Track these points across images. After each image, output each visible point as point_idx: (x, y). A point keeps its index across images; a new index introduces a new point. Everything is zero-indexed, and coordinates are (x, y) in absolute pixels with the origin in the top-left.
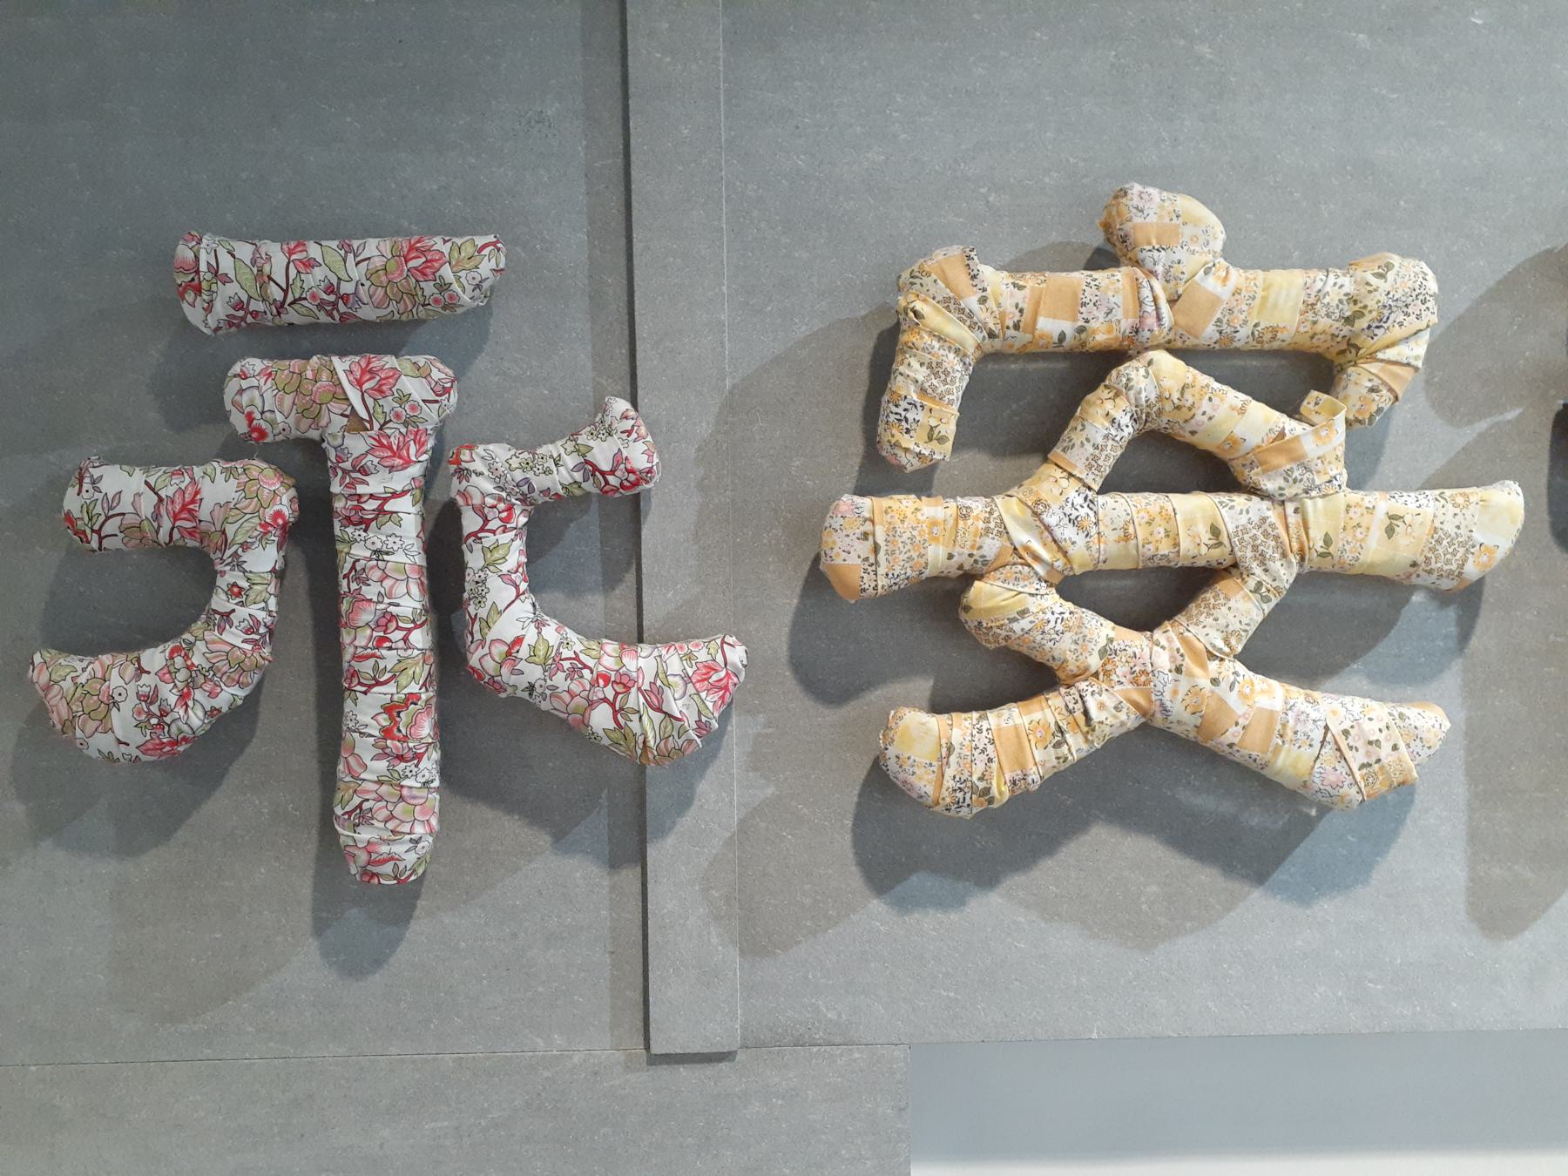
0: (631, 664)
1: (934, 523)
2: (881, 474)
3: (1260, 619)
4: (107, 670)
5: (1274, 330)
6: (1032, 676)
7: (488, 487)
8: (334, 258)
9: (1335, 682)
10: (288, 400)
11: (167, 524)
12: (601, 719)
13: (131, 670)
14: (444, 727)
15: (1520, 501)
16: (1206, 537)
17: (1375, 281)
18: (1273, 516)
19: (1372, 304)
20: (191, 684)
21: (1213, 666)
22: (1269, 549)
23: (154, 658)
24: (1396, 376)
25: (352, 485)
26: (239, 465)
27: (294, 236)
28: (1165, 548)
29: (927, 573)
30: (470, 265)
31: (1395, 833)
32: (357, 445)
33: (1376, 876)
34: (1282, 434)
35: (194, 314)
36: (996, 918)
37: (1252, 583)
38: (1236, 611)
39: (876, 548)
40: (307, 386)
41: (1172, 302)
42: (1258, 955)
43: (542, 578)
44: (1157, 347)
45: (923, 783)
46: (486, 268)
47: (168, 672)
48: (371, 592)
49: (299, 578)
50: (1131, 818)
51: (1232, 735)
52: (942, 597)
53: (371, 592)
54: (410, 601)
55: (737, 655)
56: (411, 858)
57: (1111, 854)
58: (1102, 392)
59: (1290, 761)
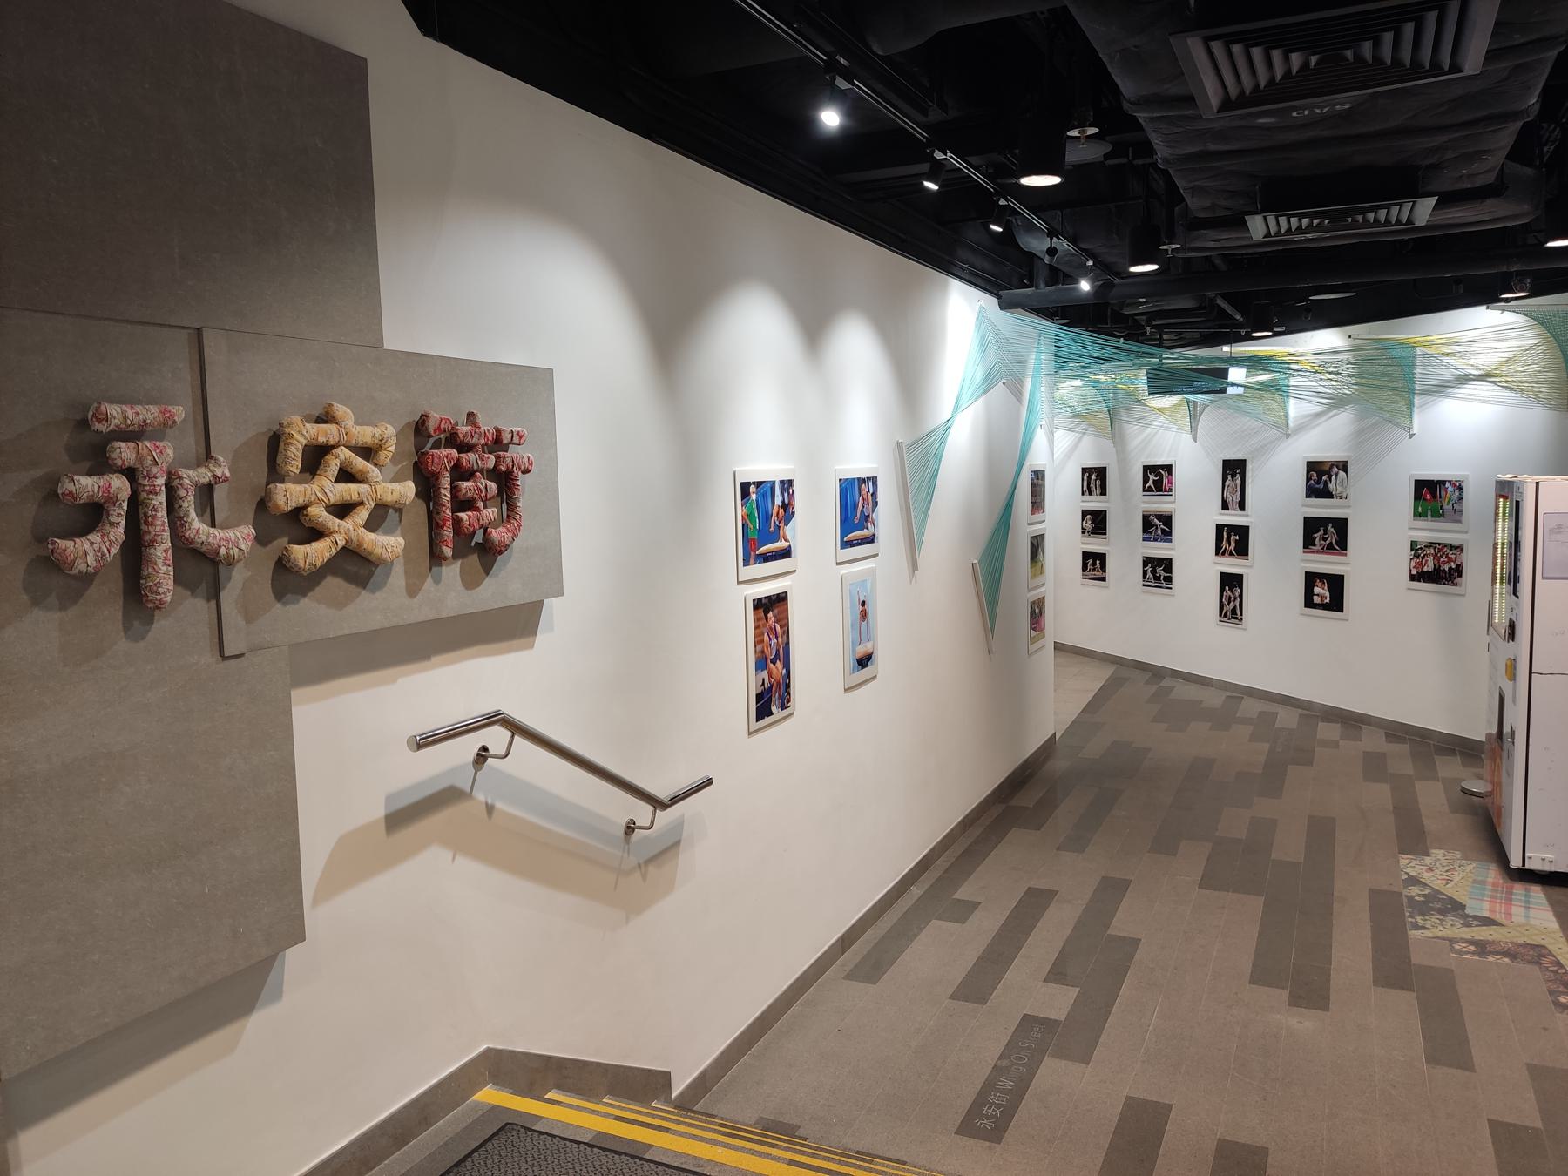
38: (362, 515)
50: (335, 574)
52: (299, 511)
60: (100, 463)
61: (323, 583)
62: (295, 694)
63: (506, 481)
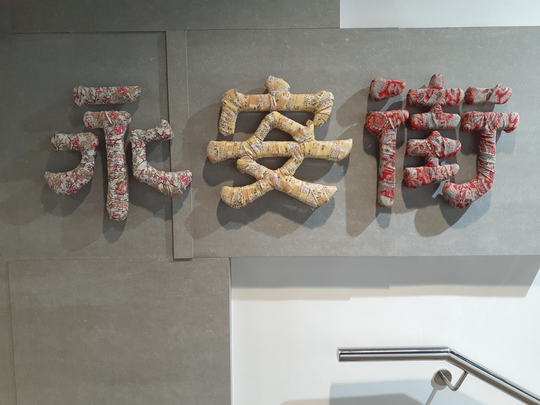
0: (167, 175)
1: (229, 147)
2: (221, 137)
3: (297, 168)
4: (60, 175)
5: (298, 107)
6: (252, 179)
7: (137, 138)
8: (105, 91)
9: (317, 181)
10: (96, 120)
11: (72, 145)
12: (161, 186)
13: (65, 175)
14: (130, 190)
15: (352, 142)
16: (284, 150)
17: (318, 97)
18: (298, 146)
19: (318, 101)
20: (77, 178)
21: (286, 177)
22: (297, 152)
23: (70, 173)
24: (324, 116)
25: (109, 138)
26: (86, 133)
27: (97, 87)
28: (276, 153)
29: (228, 157)
30: (133, 92)
31: (330, 214)
32: (110, 129)
33: (327, 223)
34: (300, 129)
35: (77, 102)
36: (247, 231)
37: (294, 160)
38: (292, 166)
39: (217, 152)
40: (100, 117)
41: (277, 101)
42: (303, 240)
43: (149, 157)
44: (275, 110)
45: (228, 201)
46: (136, 93)
47: (72, 176)
48: (113, 160)
49: (99, 158)
50: (275, 210)
51: (291, 191)
53: (113, 160)
54: (121, 162)
55: (190, 174)
56: (122, 215)
57: (271, 218)
58: (264, 120)
59: (302, 196)
60: (77, 125)
61: (262, 217)
62: (234, 292)
63: (476, 142)
